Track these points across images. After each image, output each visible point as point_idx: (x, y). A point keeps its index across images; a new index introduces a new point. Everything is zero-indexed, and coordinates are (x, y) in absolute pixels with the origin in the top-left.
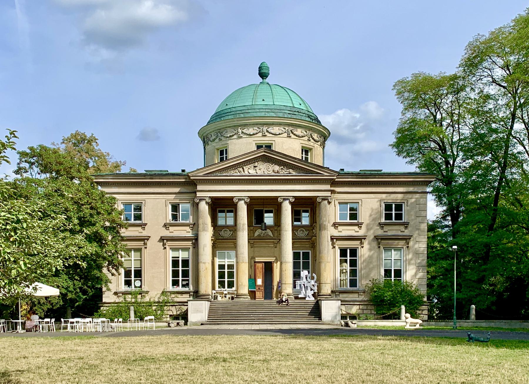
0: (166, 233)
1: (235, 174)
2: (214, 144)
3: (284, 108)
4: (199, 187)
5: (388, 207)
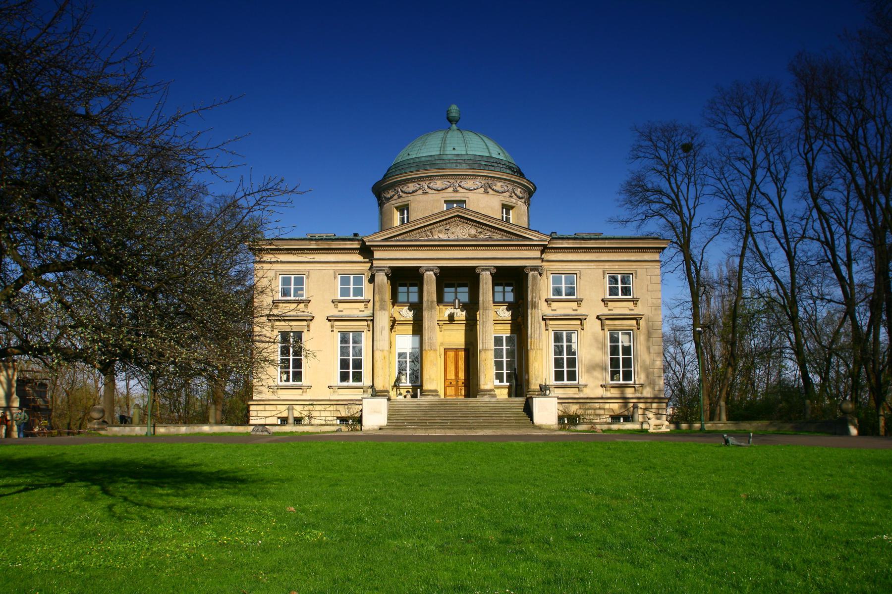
0: (334, 312)
1: (422, 238)
4: (377, 255)
5: (614, 280)
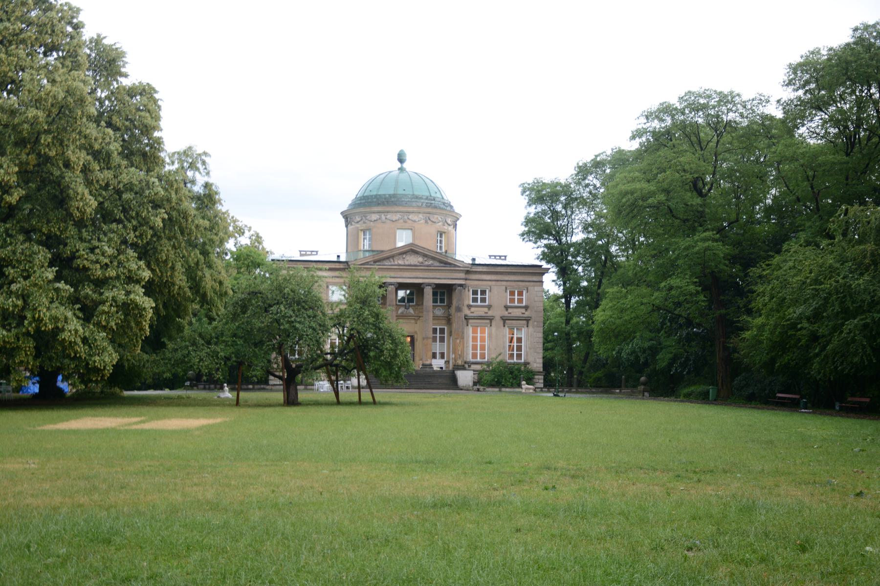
2: (358, 225)
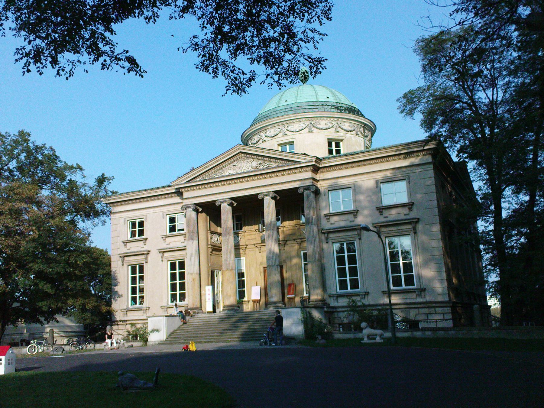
0: (164, 246)
3: (306, 104)
4: (185, 195)
